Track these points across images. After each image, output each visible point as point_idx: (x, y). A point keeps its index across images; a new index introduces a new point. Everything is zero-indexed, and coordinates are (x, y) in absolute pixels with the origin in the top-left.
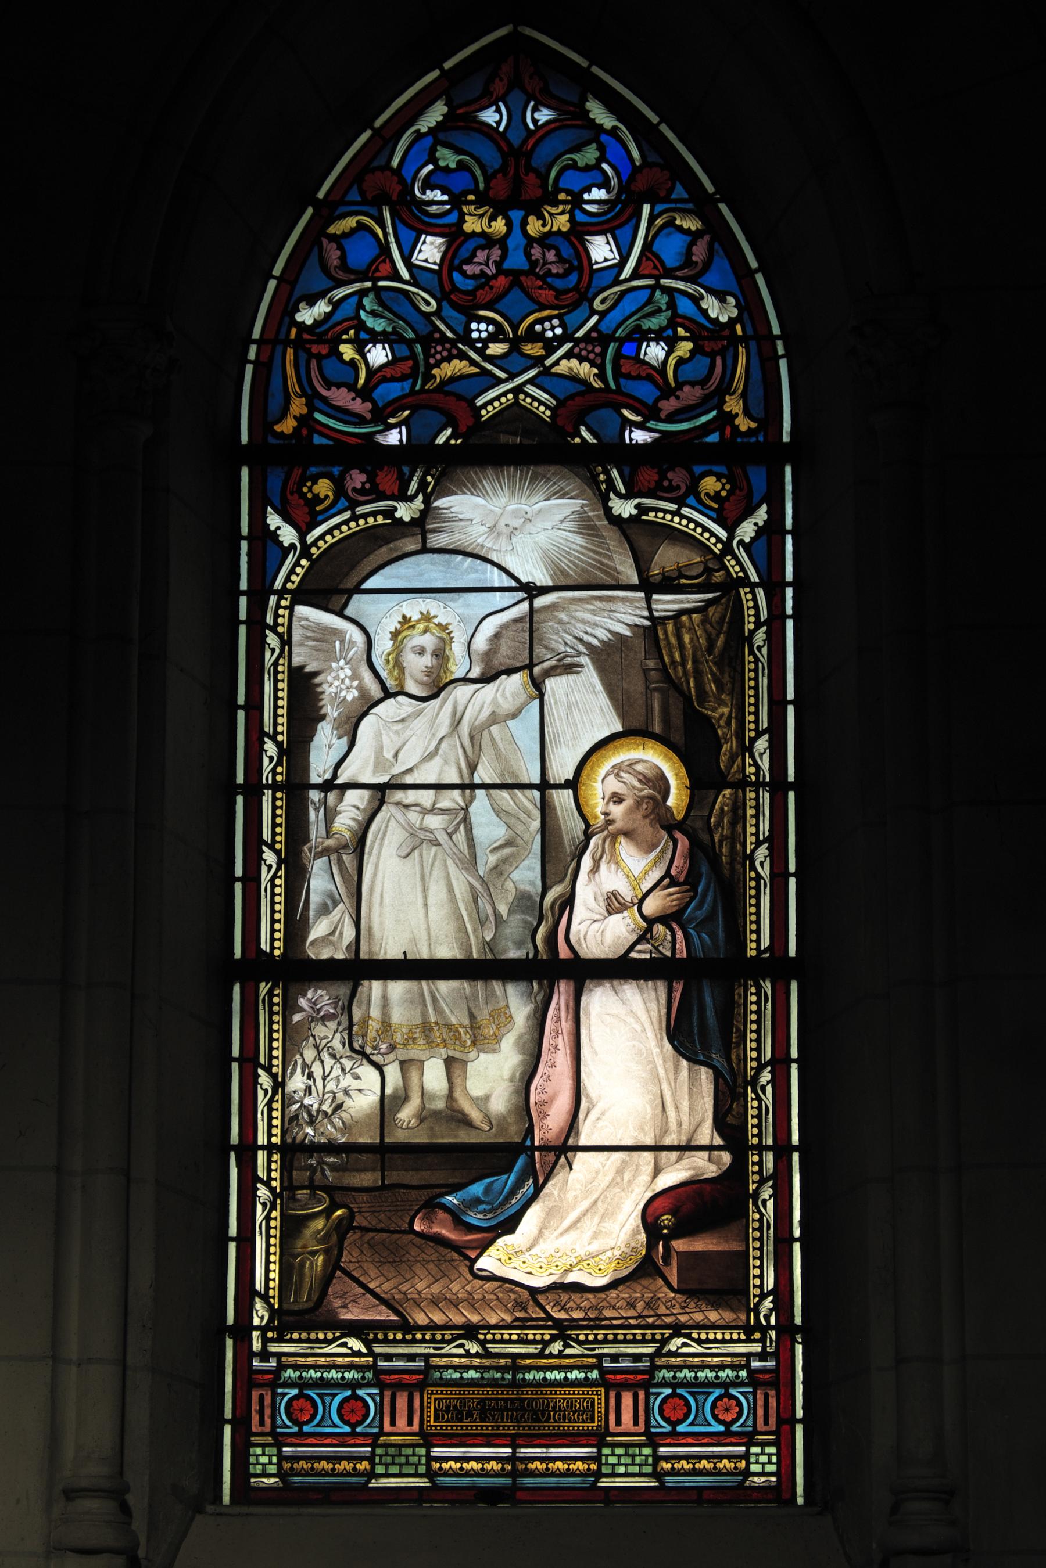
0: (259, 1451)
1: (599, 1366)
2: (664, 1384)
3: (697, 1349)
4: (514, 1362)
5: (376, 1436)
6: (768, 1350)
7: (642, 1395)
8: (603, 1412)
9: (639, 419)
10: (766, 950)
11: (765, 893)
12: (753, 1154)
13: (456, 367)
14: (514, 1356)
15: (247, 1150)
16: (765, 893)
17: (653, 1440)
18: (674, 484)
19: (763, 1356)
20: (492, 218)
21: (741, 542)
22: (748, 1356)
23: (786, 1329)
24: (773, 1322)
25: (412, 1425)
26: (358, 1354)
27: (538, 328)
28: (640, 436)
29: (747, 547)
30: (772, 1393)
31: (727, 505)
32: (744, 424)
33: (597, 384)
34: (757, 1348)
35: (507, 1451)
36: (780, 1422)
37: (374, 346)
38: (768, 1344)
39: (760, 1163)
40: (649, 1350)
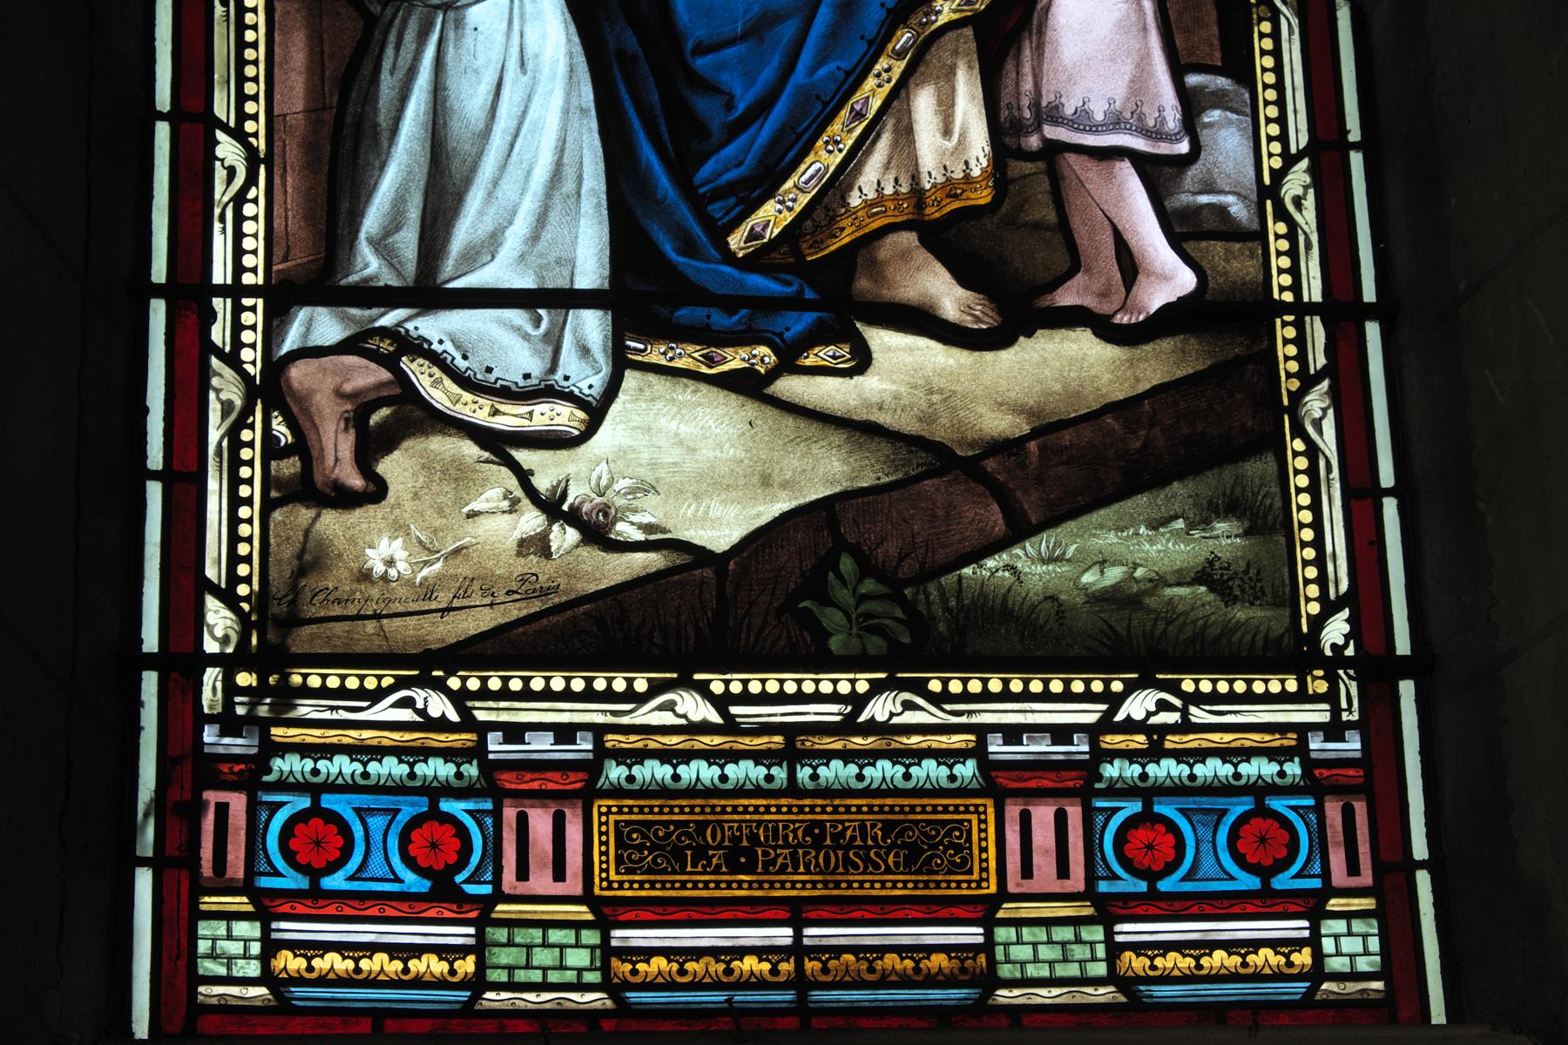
1: (978, 752)
4: (790, 741)
5: (488, 903)
6: (1345, 716)
7: (1074, 813)
12: (1284, 324)
14: (791, 731)
17: (1109, 911)
19: (1334, 730)
22: (1303, 729)
25: (564, 880)
30: (1360, 808)
34: (1317, 714)
35: (782, 935)
38: (1344, 705)
40: (1089, 714)
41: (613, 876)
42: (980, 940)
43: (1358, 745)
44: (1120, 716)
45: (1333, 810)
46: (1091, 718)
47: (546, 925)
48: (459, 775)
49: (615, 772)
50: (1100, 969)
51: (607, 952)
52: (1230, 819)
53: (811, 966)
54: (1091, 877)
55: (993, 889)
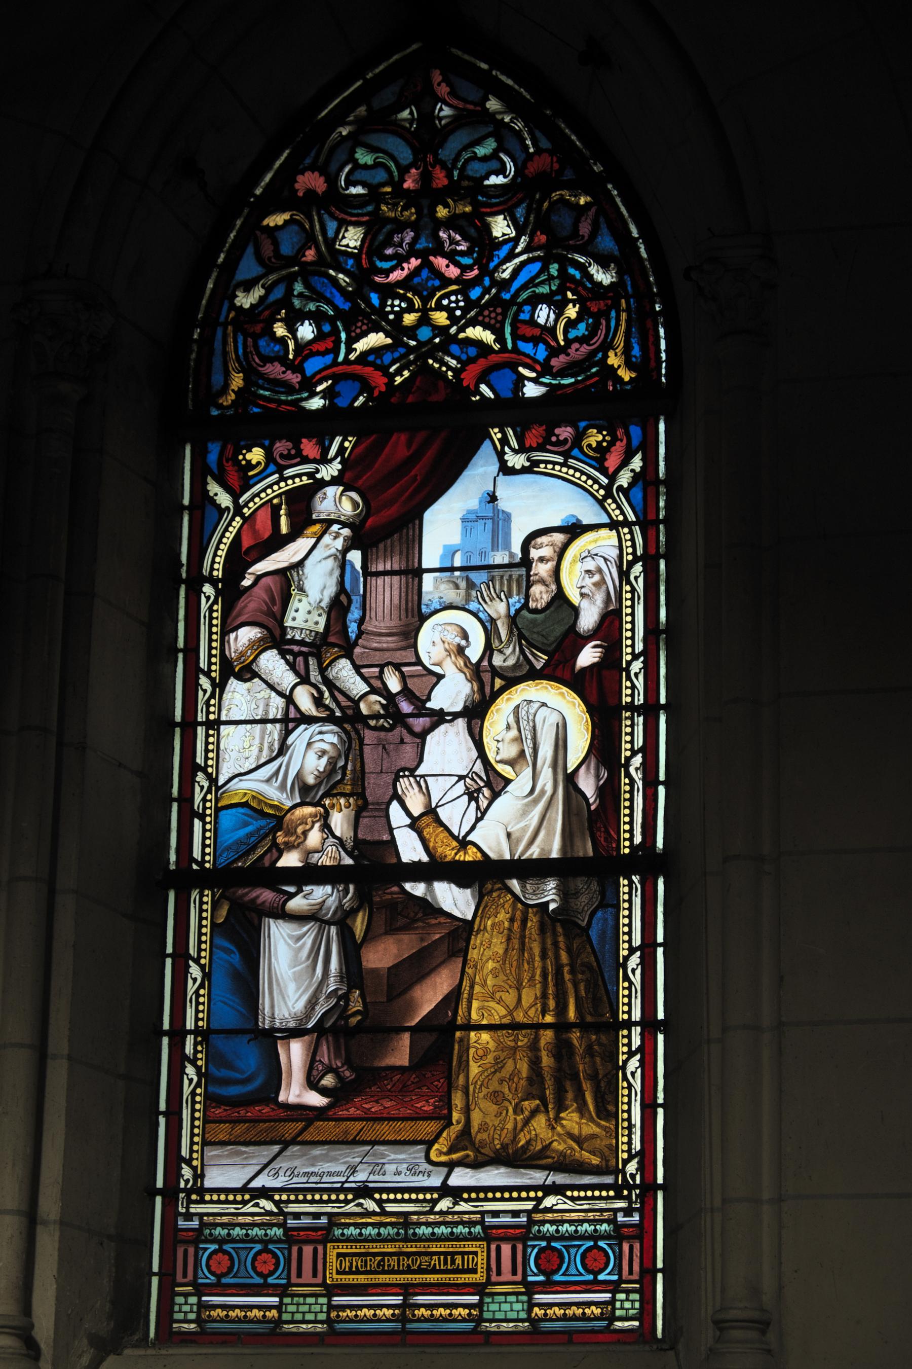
2: (541, 1237)
3: (569, 1205)
7: (520, 1247)
9: (534, 375)
13: (375, 339)
15: (178, 1034)
17: (531, 1289)
19: (628, 1212)
20: (405, 208)
22: (615, 1211)
23: (649, 1188)
27: (445, 302)
28: (531, 390)
30: (637, 1246)
32: (626, 375)
33: (497, 347)
36: (643, 1271)
37: (302, 325)
44: (541, 1207)
45: (626, 1247)
46: (530, 1207)
47: (305, 1296)
50: (523, 1315)
54: (525, 1275)
55: (484, 1281)
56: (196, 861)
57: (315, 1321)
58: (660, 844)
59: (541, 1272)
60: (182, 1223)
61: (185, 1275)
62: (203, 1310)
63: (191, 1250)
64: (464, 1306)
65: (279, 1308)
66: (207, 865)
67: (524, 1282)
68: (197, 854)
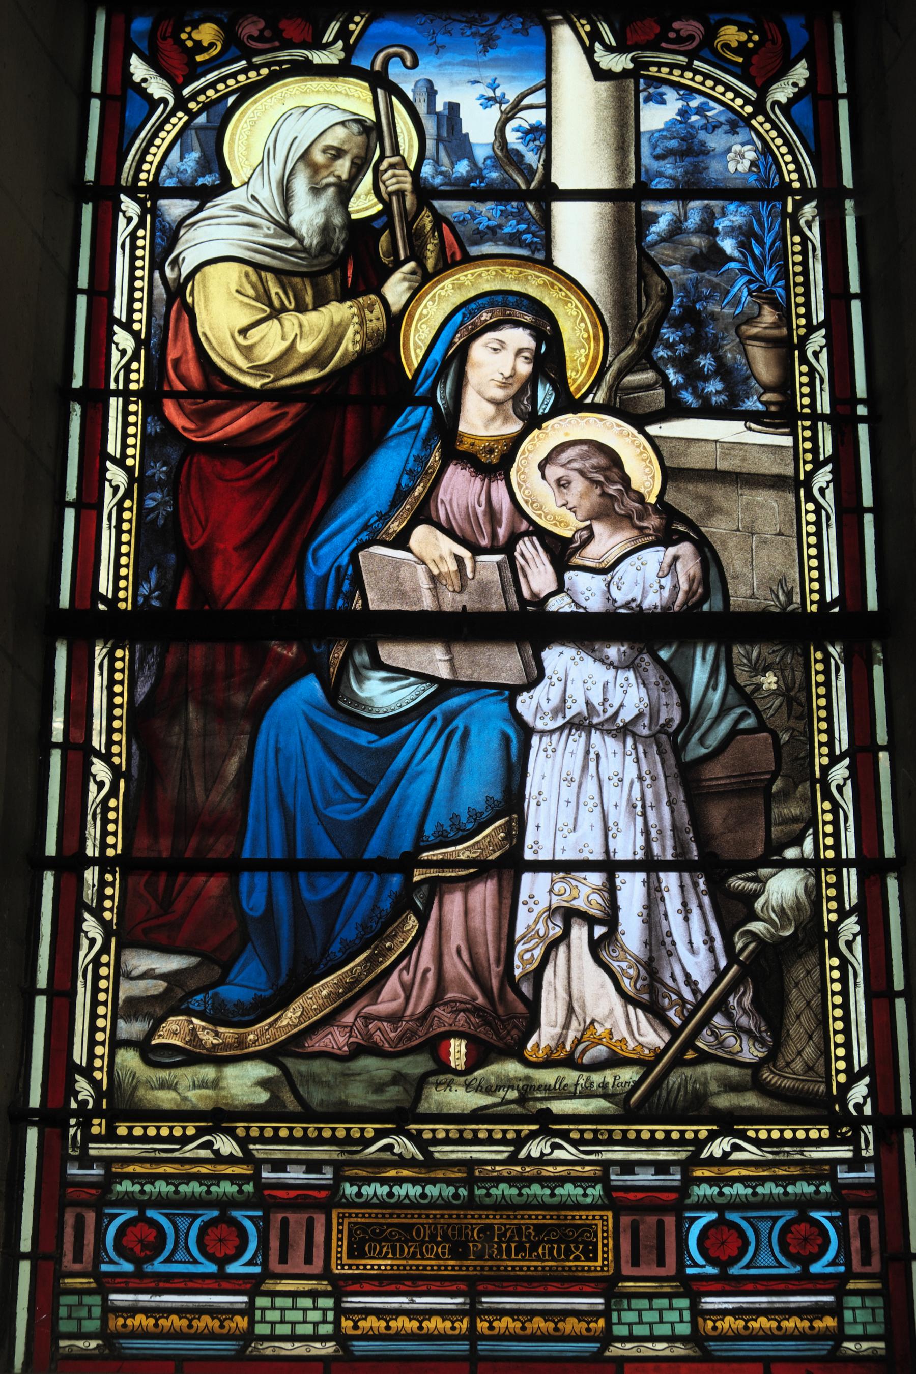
0: (73, 1299)
8: (611, 1246)
10: (834, 603)
11: (828, 526)
16: (828, 526)
18: (683, 33)
19: (856, 1163)
21: (776, 103)
22: (834, 1163)
24: (868, 1111)
26: (231, 1160)
29: (786, 109)
30: (874, 1220)
31: (755, 59)
34: (844, 1152)
38: (863, 1146)
39: (838, 885)
41: (345, 1260)
42: (601, 1307)
43: (872, 1175)
45: (853, 1220)
46: (683, 1155)
48: (240, 1191)
49: (349, 1190)
51: (340, 1312)
52: (780, 1224)
53: (482, 1326)
54: (681, 1265)
56: (104, 599)
57: (316, 1338)
58: (872, 603)
59: (711, 1260)
60: (73, 1171)
61: (78, 1257)
62: (111, 1316)
63: (90, 1217)
64: (578, 1314)
65: (249, 1311)
66: (122, 605)
67: (680, 1275)
68: (105, 586)
